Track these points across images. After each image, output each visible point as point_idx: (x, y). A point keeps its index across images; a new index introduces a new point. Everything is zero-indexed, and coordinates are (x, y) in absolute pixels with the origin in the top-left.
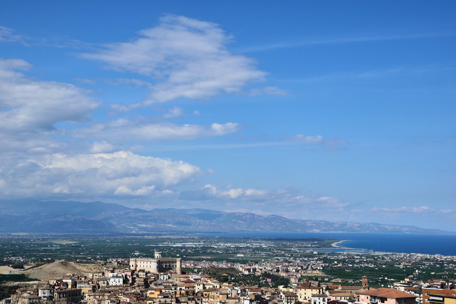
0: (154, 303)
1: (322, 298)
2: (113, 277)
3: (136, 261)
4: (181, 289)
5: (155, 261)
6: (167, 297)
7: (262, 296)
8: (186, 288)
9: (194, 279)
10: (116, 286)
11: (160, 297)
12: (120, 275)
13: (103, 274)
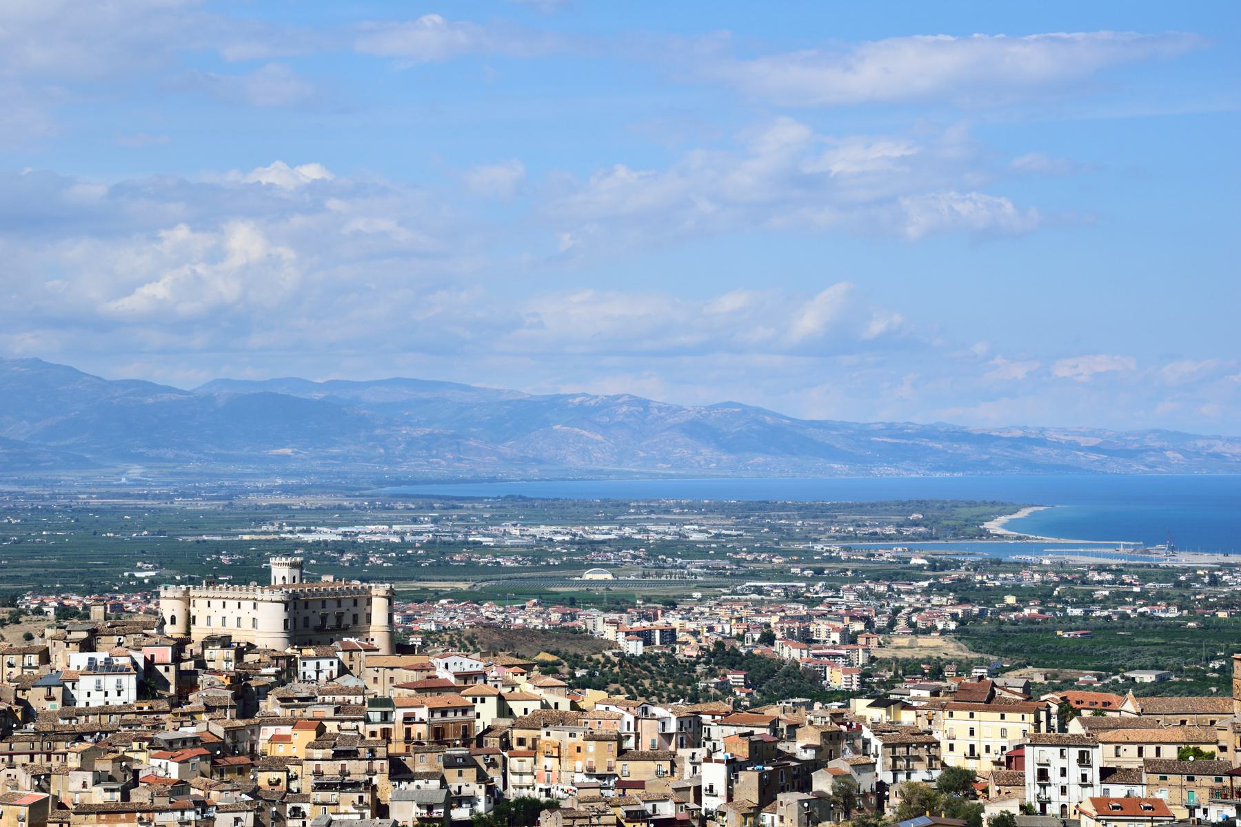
0: (289, 780)
1: (1073, 753)
2: (92, 668)
3: (187, 600)
4: (408, 719)
5: (278, 596)
6: (351, 754)
7: (781, 746)
8: (432, 711)
9: (457, 676)
10: (105, 711)
11: (318, 754)
12: (124, 661)
13: (45, 657)
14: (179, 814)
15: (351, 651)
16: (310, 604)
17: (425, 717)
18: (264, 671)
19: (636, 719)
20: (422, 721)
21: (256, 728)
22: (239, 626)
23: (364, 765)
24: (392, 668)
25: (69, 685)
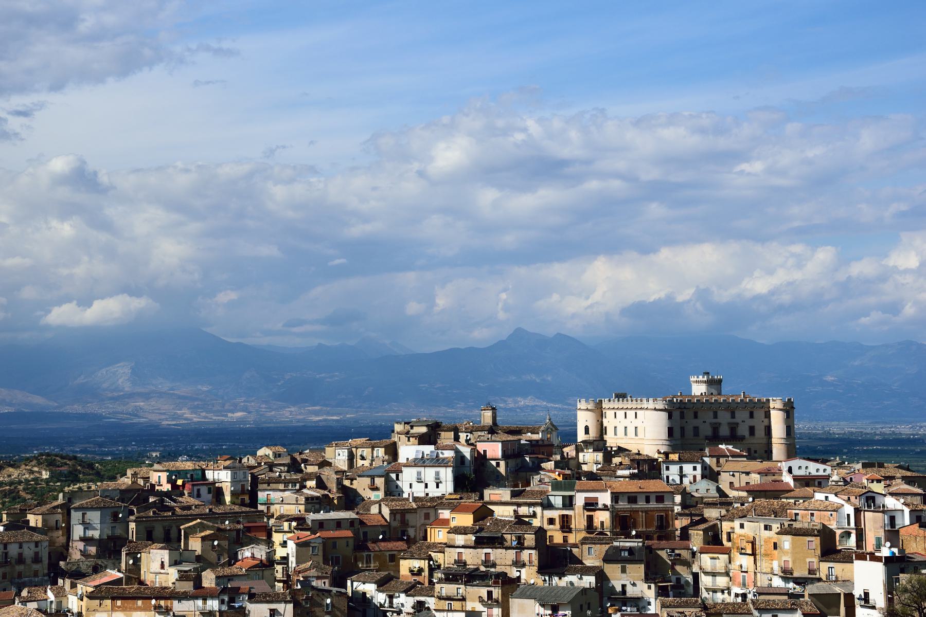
0: (431, 570)
2: (420, 462)
4: (591, 505)
6: (496, 542)
8: (616, 497)
9: (796, 479)
11: (460, 539)
12: (449, 454)
14: (200, 602)
15: (718, 458)
16: (699, 414)
17: (608, 502)
18: (620, 473)
19: (857, 511)
20: (605, 508)
21: (432, 512)
22: (636, 435)
23: (511, 554)
24: (748, 473)
25: (393, 476)
